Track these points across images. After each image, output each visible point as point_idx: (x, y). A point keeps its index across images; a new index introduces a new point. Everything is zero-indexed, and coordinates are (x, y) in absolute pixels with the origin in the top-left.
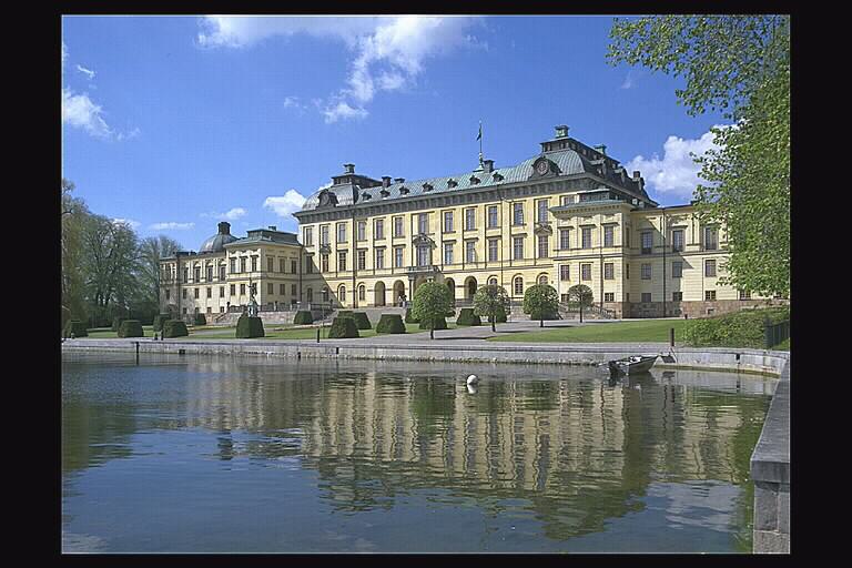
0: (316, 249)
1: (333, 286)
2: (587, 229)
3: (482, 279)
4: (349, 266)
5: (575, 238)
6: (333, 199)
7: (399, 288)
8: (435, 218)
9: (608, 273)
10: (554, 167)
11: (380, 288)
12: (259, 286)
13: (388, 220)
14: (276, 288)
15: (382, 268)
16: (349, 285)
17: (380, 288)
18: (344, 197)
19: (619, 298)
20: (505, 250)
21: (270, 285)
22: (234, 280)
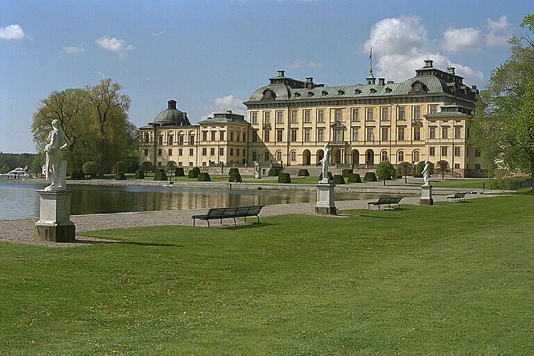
0: (260, 127)
1: (273, 151)
2: (445, 128)
4: (285, 138)
5: (438, 133)
6: (274, 95)
7: (320, 155)
8: (346, 112)
9: (457, 152)
10: (424, 87)
11: (307, 155)
12: (225, 150)
13: (314, 111)
14: (235, 152)
15: (308, 141)
16: (284, 151)
17: (307, 155)
18: (281, 93)
19: (462, 166)
20: (393, 135)
21: (232, 150)
22: (206, 145)
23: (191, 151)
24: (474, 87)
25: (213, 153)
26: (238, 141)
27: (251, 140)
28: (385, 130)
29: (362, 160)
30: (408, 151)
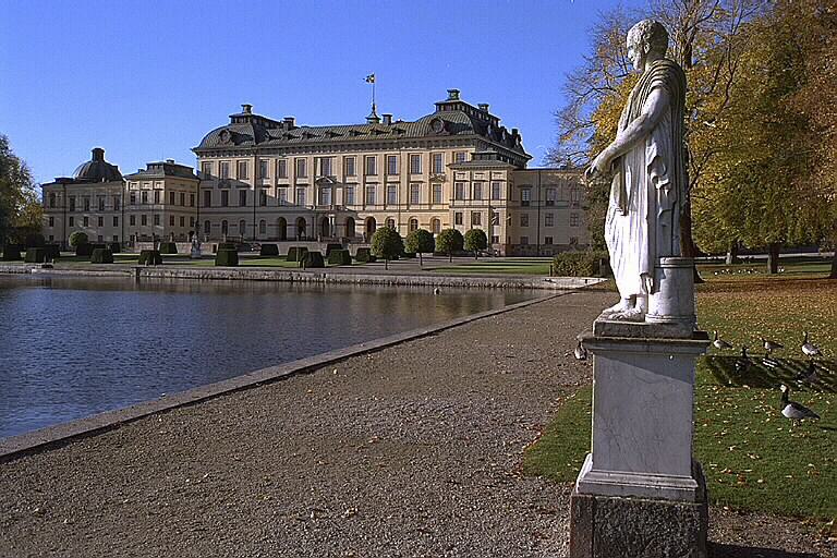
3: (380, 221)
12: (161, 218)
14: (177, 222)
19: (502, 240)
20: (402, 194)
21: (172, 217)
25: (144, 222)
26: (182, 204)
27: (202, 204)
28: (390, 191)
29: (360, 230)
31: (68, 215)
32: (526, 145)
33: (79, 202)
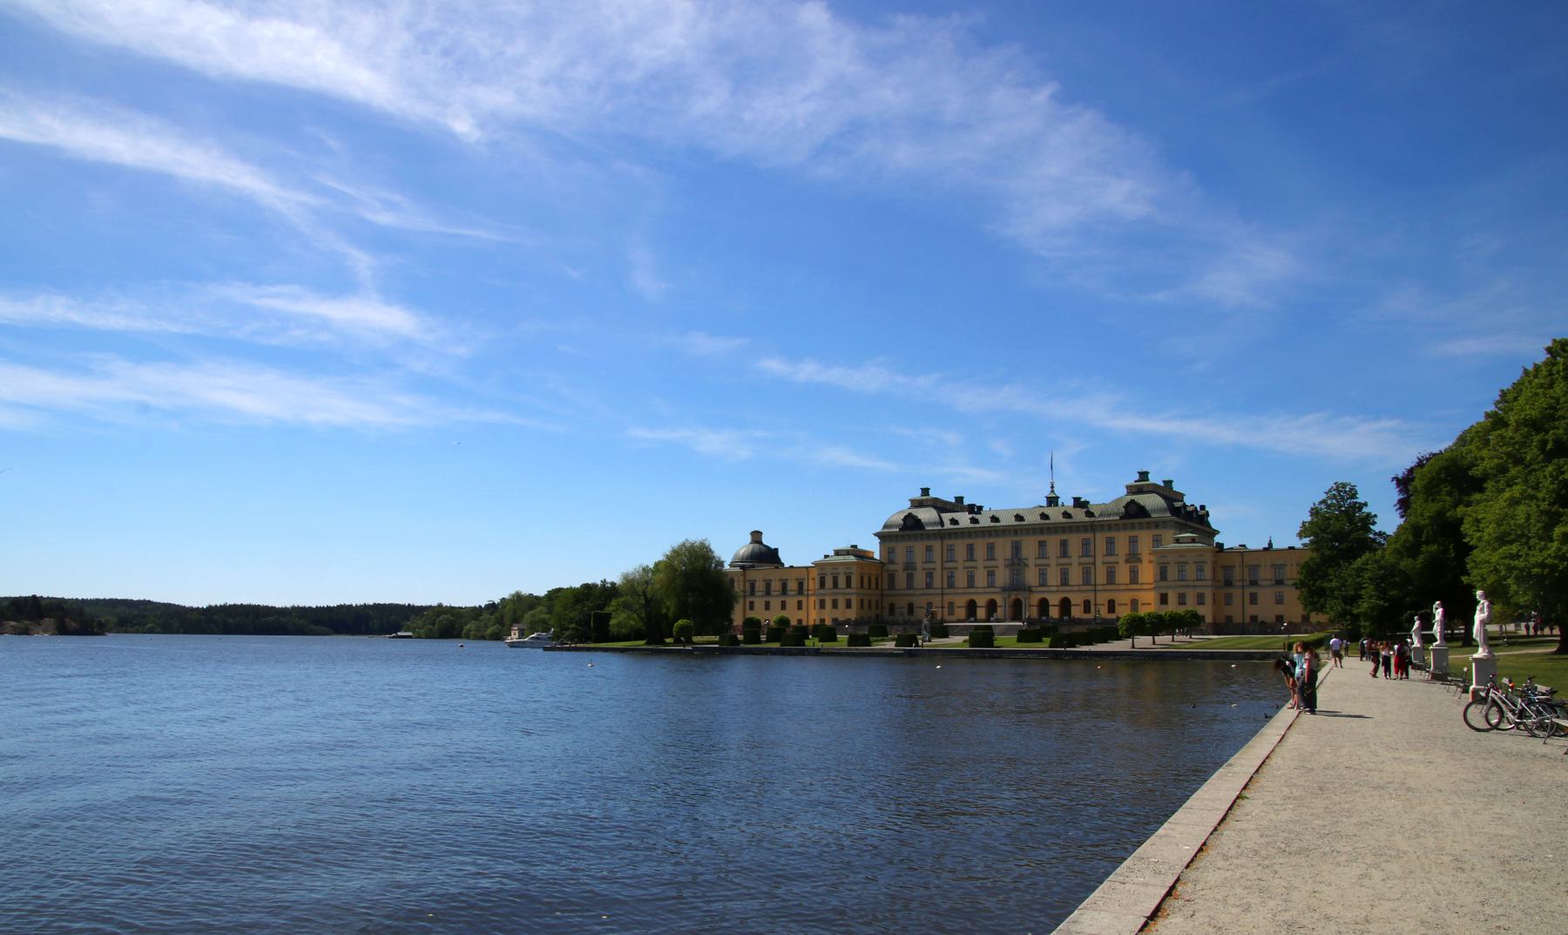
3: (1077, 599)
4: (937, 582)
17: (972, 607)
20: (1101, 577)
23: (800, 603)
24: (1203, 507)
27: (886, 586)
28: (1087, 574)
29: (1054, 613)
30: (1123, 598)
31: (749, 600)
32: (1213, 521)
33: (760, 586)
